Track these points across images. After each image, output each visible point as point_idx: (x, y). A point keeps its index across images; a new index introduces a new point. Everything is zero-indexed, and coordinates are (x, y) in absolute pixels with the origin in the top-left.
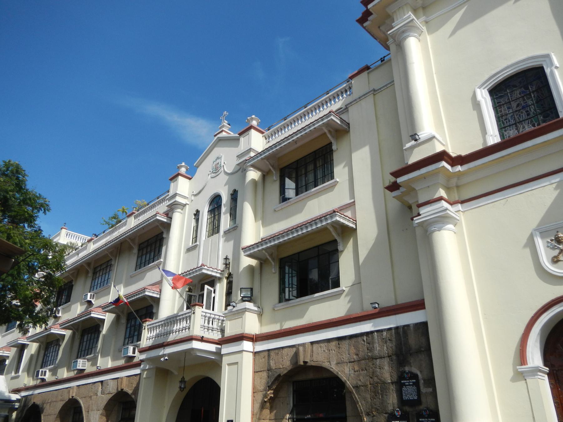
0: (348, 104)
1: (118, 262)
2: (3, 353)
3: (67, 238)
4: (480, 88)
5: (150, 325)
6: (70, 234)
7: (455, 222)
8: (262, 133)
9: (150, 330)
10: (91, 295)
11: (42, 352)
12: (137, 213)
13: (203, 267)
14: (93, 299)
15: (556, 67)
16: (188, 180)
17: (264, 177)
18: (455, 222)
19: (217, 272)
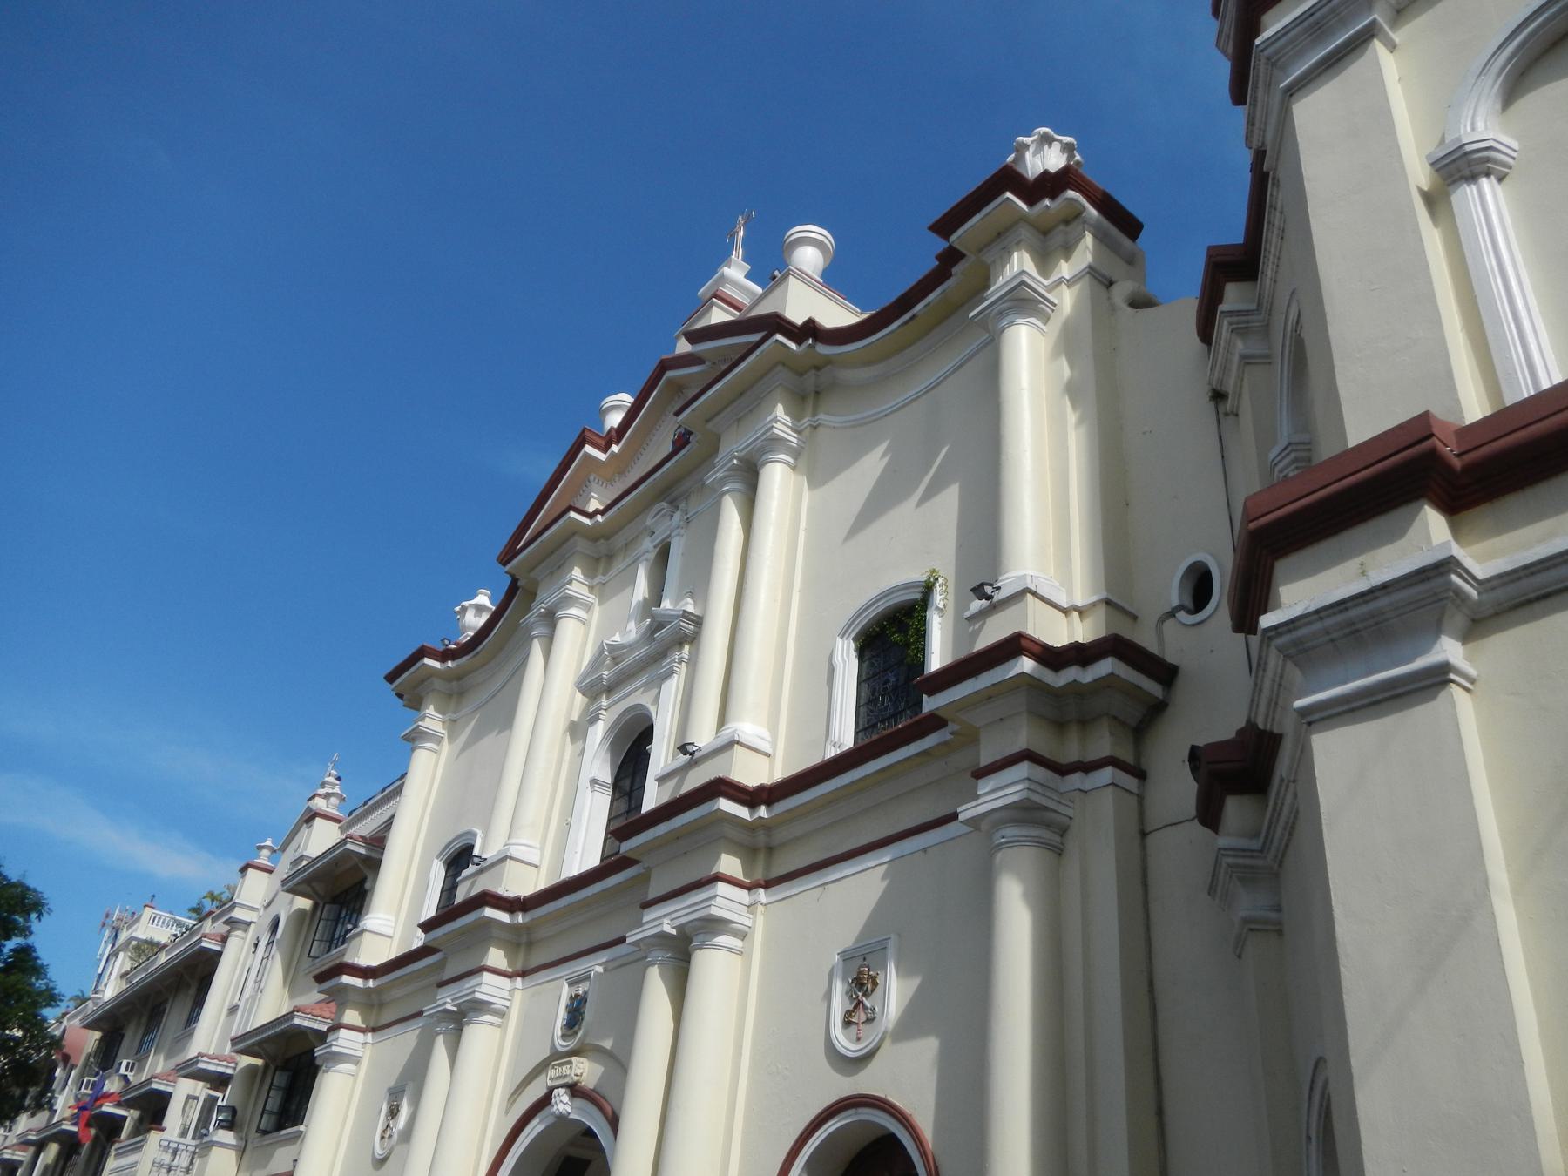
1: (171, 1007)
2: (13, 1154)
3: (154, 926)
4: (437, 858)
5: (119, 1149)
6: (160, 918)
7: (356, 1061)
8: (338, 821)
9: (118, 1156)
10: (128, 1063)
11: (61, 1163)
12: (218, 912)
13: (199, 1058)
14: (131, 1071)
16: (266, 875)
17: (315, 907)
18: (356, 1061)
19: (227, 1067)
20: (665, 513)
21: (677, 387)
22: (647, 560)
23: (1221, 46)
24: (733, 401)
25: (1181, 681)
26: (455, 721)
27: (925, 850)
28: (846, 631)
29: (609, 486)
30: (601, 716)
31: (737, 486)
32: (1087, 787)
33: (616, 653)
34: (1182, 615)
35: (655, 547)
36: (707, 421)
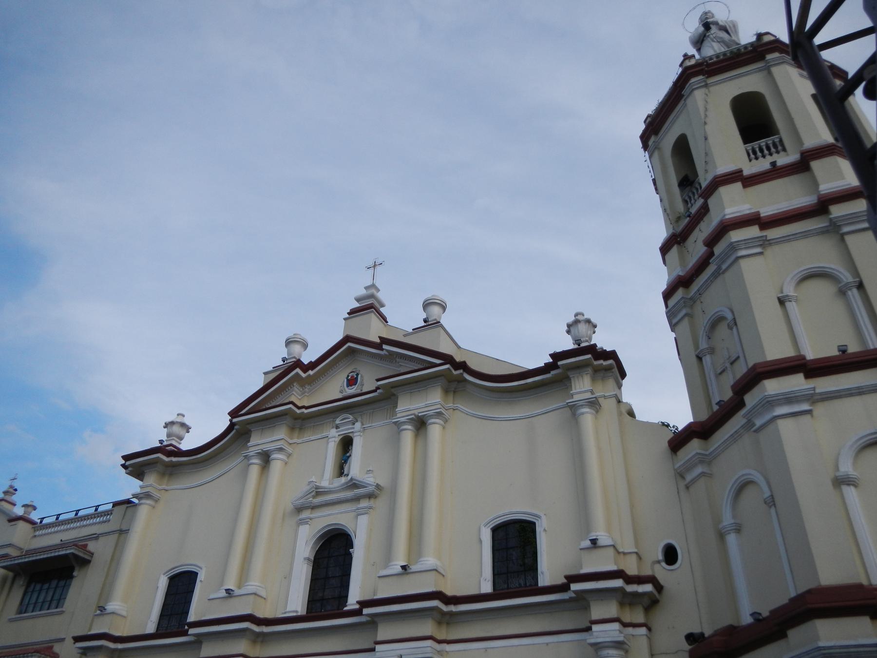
0: (100, 534)
4: (164, 574)
15: (201, 581)
20: (350, 421)
21: (352, 351)
22: (335, 441)
23: (668, 315)
24: (410, 384)
25: (665, 592)
26: (167, 490)
27: (547, 644)
28: (487, 525)
29: (301, 390)
30: (309, 523)
31: (410, 427)
32: (634, 634)
33: (318, 492)
34: (664, 564)
35: (339, 435)
36: (392, 387)
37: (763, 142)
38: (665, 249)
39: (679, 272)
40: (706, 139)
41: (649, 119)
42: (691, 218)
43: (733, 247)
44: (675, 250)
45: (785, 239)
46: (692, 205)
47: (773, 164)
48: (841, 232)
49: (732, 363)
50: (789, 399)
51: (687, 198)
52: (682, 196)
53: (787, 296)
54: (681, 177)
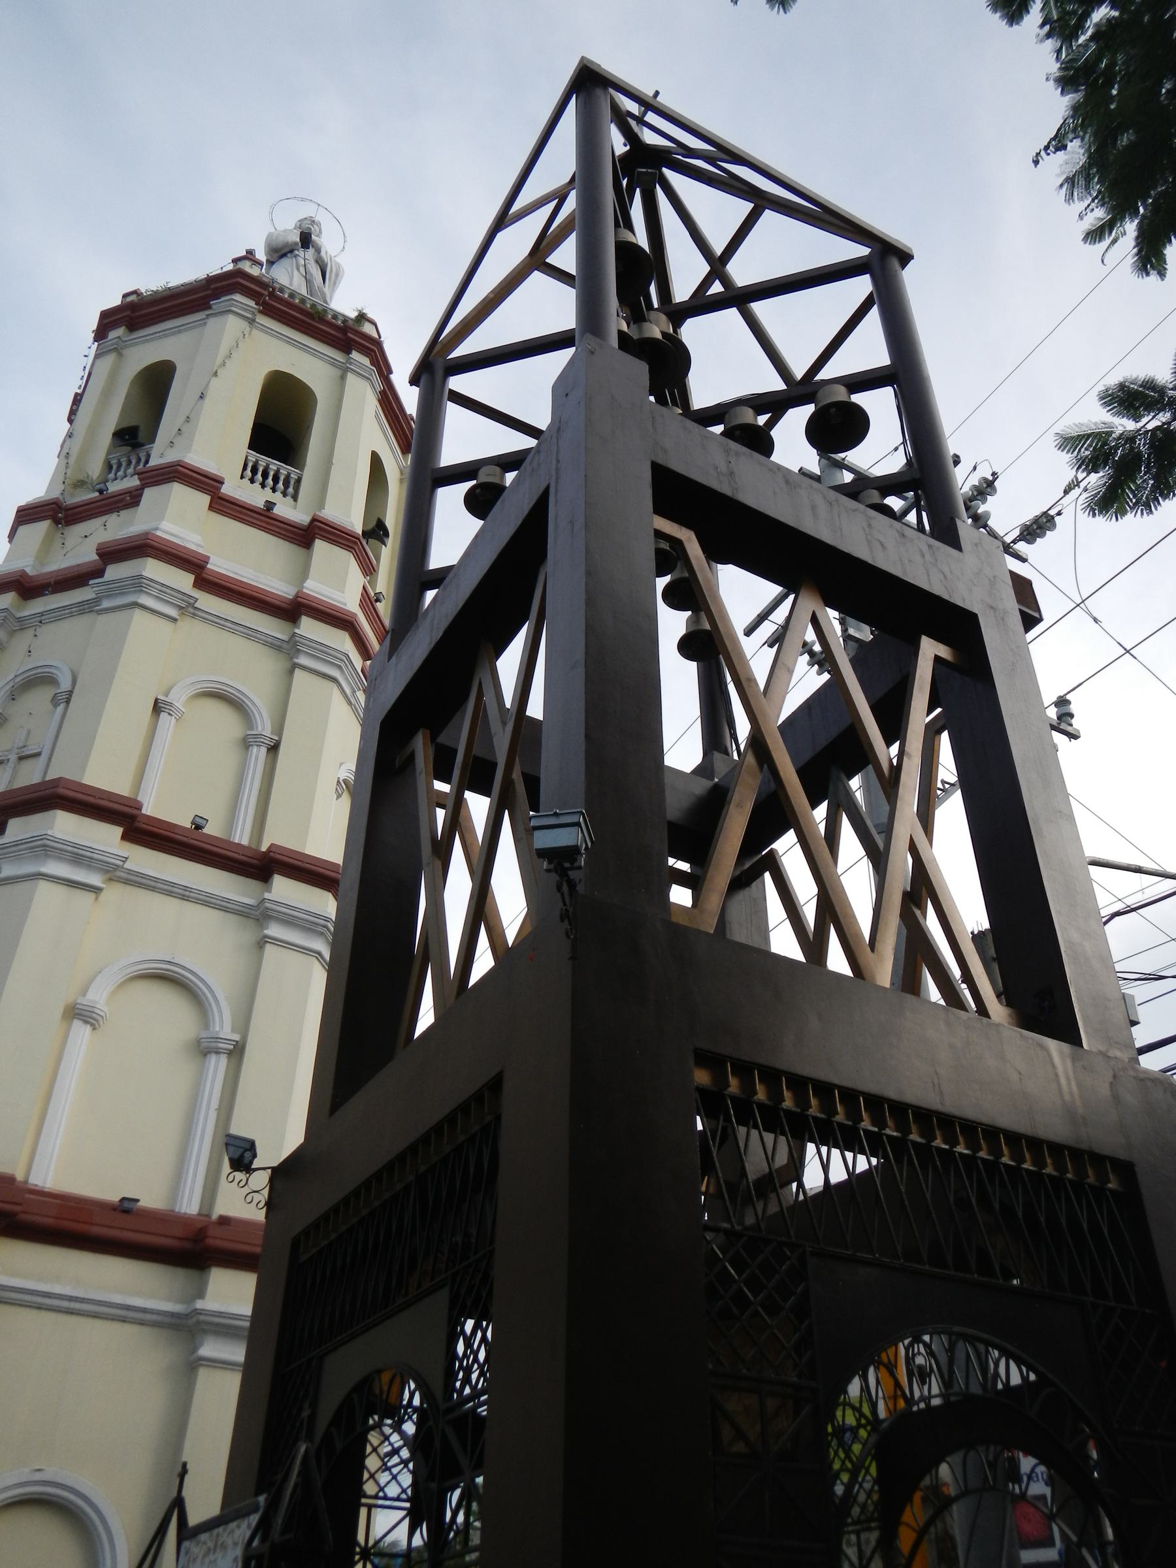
37: (274, 465)
38: (27, 515)
39: (28, 566)
40: (202, 397)
41: (133, 298)
42: (102, 497)
43: (138, 584)
44: (44, 526)
45: (216, 620)
46: (116, 479)
47: (270, 505)
48: (295, 660)
49: (21, 758)
50: (79, 856)
51: (114, 462)
52: (108, 453)
53: (171, 704)
54: (124, 425)
